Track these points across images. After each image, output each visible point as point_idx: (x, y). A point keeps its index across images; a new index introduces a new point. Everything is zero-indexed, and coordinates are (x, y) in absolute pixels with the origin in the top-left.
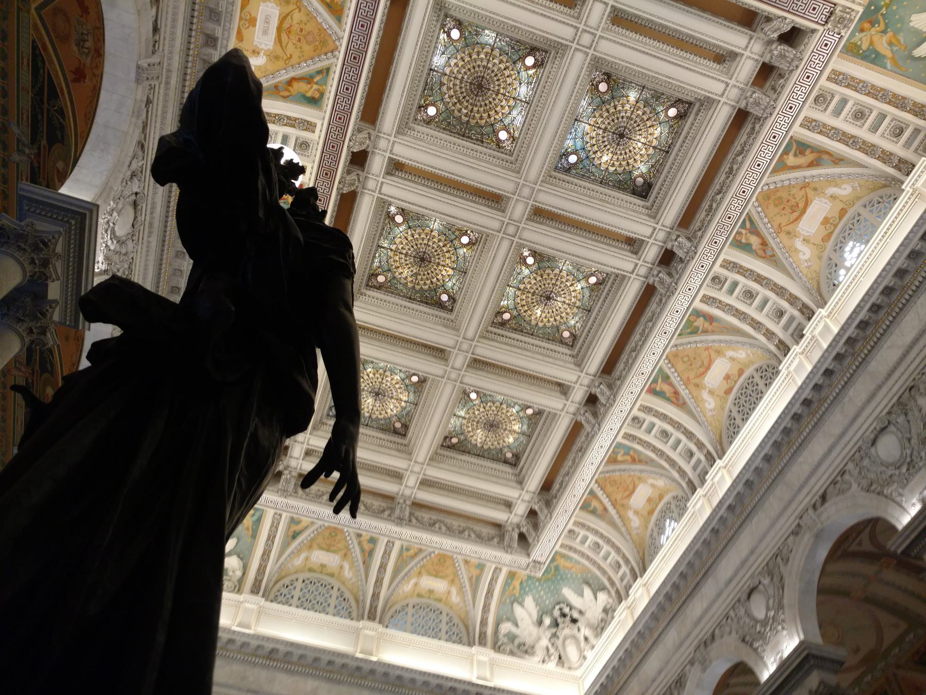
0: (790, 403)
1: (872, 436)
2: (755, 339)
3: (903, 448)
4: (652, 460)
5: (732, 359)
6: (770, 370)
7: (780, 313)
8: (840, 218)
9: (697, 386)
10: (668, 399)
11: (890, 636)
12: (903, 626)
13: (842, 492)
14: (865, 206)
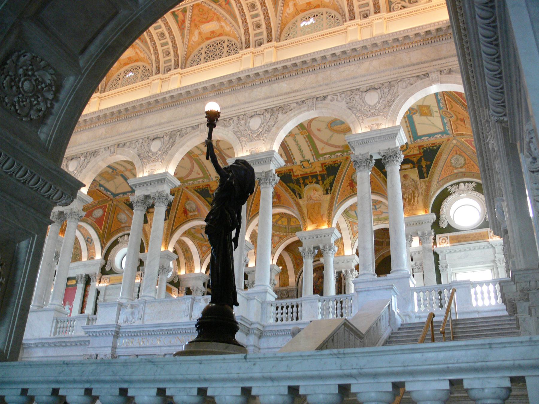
0: (233, 74)
1: (253, 114)
2: (239, 27)
3: (260, 128)
4: (146, 42)
5: (222, 27)
6: (234, 46)
7: (259, 26)
8: (315, 8)
9: (196, 25)
10: (177, 21)
11: (193, 176)
12: (201, 175)
13: (225, 126)
14: (327, 13)
